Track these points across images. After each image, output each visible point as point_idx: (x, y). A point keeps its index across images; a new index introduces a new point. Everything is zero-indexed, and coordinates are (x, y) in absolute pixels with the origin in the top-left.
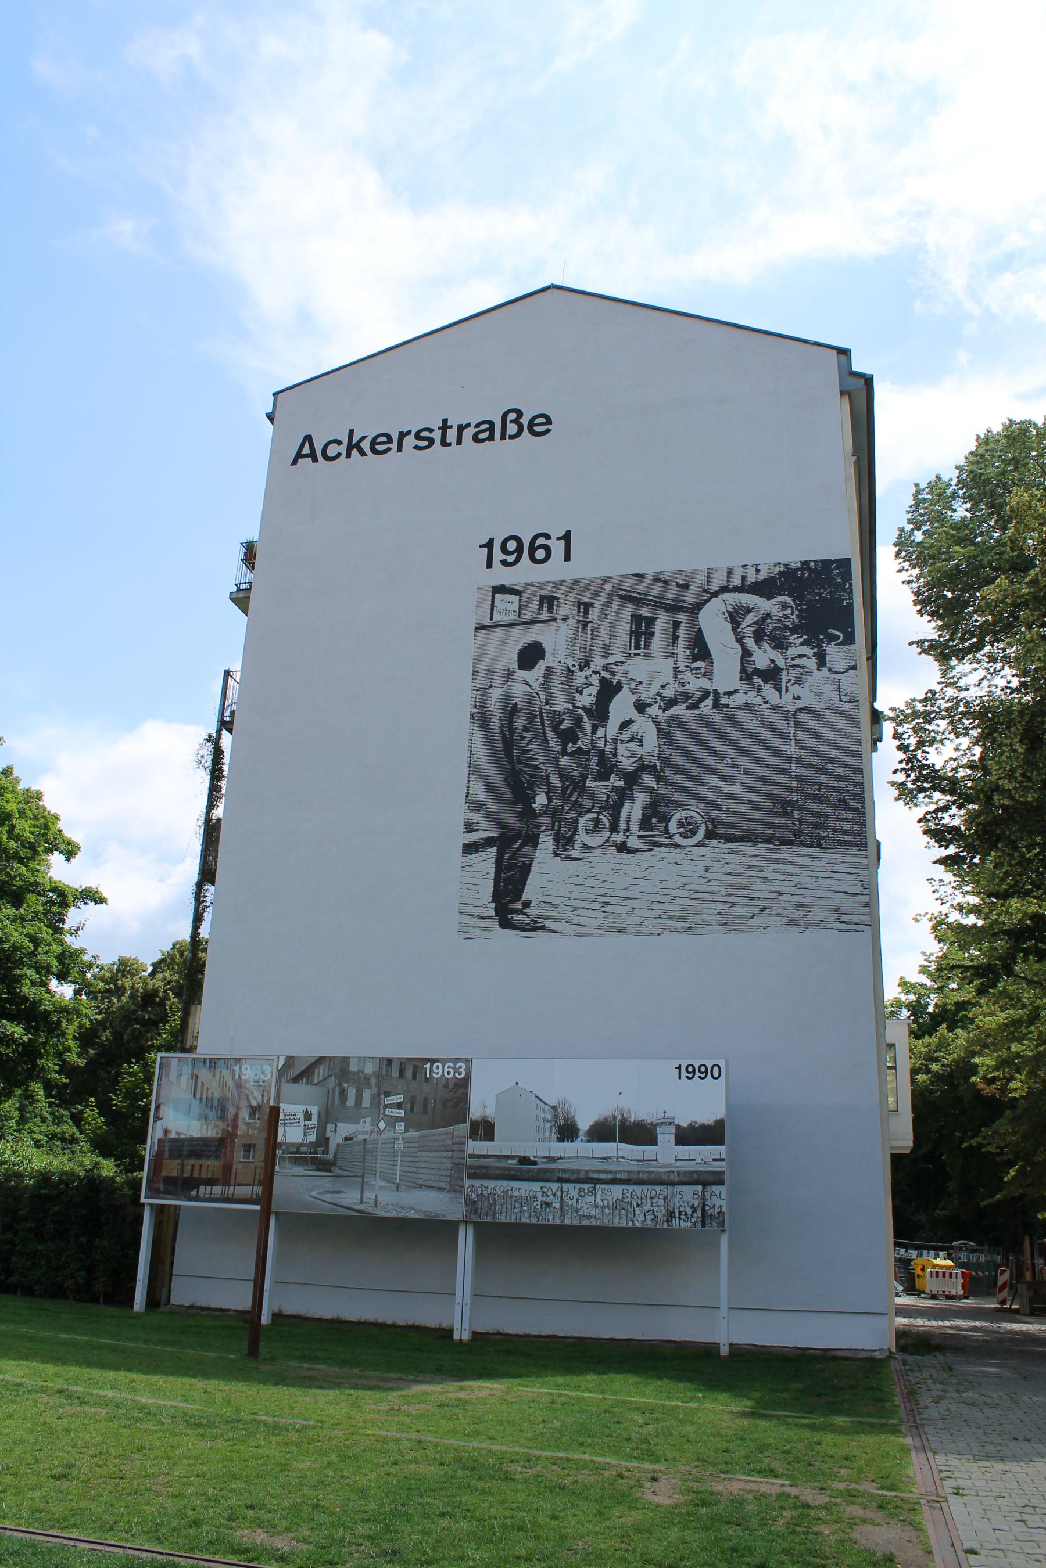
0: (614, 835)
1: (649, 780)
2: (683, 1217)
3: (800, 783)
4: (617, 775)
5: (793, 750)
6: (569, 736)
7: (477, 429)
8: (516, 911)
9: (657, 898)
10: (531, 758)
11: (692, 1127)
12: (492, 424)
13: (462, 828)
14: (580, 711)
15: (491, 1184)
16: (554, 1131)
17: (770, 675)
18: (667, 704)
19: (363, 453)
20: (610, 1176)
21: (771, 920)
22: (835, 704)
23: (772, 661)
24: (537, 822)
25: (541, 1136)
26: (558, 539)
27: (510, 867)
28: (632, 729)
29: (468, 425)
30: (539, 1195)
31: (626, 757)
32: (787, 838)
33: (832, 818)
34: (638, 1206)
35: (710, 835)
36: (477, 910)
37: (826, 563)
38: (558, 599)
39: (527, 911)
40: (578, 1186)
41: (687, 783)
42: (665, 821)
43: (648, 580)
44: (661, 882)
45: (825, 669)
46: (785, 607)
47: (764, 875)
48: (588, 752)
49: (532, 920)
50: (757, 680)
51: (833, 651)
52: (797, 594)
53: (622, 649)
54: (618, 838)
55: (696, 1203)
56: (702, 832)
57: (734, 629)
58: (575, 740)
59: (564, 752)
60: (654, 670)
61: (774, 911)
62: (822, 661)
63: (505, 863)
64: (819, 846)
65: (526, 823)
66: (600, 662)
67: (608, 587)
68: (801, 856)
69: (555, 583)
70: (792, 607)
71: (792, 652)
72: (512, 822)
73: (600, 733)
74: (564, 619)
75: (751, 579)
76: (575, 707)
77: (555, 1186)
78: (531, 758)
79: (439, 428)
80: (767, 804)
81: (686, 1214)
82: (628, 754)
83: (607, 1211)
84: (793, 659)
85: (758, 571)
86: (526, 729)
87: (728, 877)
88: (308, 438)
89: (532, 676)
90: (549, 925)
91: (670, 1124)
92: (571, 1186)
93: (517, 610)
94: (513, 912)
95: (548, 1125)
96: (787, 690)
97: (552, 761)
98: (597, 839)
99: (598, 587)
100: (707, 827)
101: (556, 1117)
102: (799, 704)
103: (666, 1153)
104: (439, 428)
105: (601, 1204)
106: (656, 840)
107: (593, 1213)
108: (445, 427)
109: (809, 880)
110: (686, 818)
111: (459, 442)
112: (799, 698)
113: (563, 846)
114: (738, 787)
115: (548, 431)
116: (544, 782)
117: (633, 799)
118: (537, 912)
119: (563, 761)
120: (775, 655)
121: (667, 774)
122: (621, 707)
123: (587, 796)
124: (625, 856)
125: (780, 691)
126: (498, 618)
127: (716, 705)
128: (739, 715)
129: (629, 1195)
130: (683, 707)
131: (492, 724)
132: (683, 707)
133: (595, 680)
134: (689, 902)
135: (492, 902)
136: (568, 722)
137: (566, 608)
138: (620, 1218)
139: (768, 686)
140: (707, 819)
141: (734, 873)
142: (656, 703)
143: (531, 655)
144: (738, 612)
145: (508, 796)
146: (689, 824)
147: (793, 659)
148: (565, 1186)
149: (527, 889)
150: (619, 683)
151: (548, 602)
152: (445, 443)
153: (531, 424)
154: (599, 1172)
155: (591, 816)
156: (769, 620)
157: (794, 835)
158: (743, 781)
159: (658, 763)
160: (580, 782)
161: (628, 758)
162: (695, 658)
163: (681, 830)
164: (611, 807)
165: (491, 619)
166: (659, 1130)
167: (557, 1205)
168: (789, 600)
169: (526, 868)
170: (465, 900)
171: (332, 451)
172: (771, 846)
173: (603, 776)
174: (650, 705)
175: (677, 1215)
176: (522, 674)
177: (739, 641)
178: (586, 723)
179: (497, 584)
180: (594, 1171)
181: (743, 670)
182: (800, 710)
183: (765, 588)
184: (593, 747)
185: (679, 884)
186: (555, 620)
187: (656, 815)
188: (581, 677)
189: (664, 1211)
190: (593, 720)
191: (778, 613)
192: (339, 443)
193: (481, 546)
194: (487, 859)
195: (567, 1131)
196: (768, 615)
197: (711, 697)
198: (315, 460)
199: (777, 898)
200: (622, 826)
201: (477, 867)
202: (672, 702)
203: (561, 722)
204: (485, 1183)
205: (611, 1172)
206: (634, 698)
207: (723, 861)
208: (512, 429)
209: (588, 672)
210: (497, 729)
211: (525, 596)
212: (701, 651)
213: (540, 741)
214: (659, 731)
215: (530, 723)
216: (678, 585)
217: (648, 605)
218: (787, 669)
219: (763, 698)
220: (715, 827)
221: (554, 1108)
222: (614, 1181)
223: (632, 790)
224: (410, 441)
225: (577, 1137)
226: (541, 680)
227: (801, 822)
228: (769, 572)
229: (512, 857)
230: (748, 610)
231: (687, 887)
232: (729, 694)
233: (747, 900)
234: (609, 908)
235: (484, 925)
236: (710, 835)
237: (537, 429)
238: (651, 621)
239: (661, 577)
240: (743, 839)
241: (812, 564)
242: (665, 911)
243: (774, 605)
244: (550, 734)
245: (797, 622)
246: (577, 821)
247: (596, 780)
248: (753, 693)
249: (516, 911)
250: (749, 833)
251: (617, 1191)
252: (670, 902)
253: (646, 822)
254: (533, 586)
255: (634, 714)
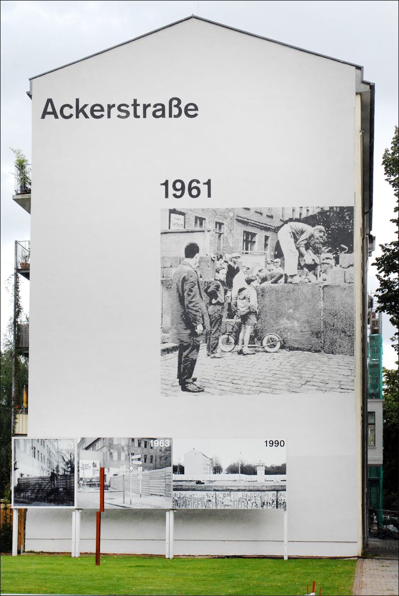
0: (237, 346)
1: (253, 319)
3: (325, 322)
4: (237, 316)
5: (322, 306)
6: (213, 295)
7: (155, 109)
8: (190, 383)
9: (257, 377)
10: (194, 306)
13: (160, 341)
14: (218, 282)
17: (312, 267)
18: (262, 280)
19: (86, 117)
21: (310, 387)
22: (343, 284)
23: (313, 260)
24: (198, 339)
26: (204, 184)
27: (186, 361)
28: (244, 293)
29: (149, 105)
31: (242, 308)
32: (318, 349)
33: (339, 340)
35: (282, 347)
36: (170, 382)
37: (342, 208)
38: (205, 219)
39: (195, 383)
41: (272, 321)
42: (261, 339)
43: (252, 211)
44: (259, 369)
45: (338, 266)
46: (321, 231)
47: (307, 366)
48: (222, 304)
49: (198, 387)
50: (306, 270)
51: (342, 256)
52: (327, 225)
53: (239, 250)
54: (238, 348)
56: (278, 345)
57: (295, 242)
58: (216, 297)
59: (210, 303)
60: (255, 262)
61: (311, 383)
62: (337, 262)
63: (183, 359)
64: (333, 353)
65: (193, 339)
66: (227, 257)
67: (231, 214)
68: (323, 357)
69: (203, 210)
70: (324, 232)
71: (323, 256)
72: (186, 339)
73: (229, 294)
74: (208, 231)
75: (304, 215)
76: (215, 280)
78: (194, 306)
79: (132, 105)
80: (309, 333)
82: (243, 306)
84: (323, 260)
85: (308, 210)
86: (191, 291)
87: (291, 367)
88: (50, 101)
89: (193, 261)
90: (206, 389)
93: (183, 224)
94: (188, 383)
96: (320, 276)
97: (204, 308)
98: (228, 348)
99: (226, 214)
100: (281, 343)
102: (326, 283)
104: (132, 105)
106: (257, 349)
109: (327, 369)
110: (271, 338)
111: (145, 116)
112: (325, 280)
113: (212, 351)
114: (296, 324)
115: (196, 115)
116: (201, 319)
117: (245, 329)
118: (200, 383)
119: (211, 308)
120: (315, 257)
121: (262, 316)
122: (239, 281)
123: (223, 326)
124: (241, 356)
125: (316, 276)
126: (173, 229)
127: (286, 282)
128: (297, 287)
130: (270, 282)
131: (172, 287)
132: (270, 282)
133: (225, 266)
134: (272, 379)
135: (178, 378)
136: (212, 288)
137: (209, 225)
139: (311, 273)
140: (281, 339)
141: (293, 366)
142: (256, 279)
143: (192, 250)
144: (297, 233)
145: (183, 326)
146: (272, 341)
147: (323, 260)
149: (194, 372)
150: (238, 268)
151: (200, 220)
155: (225, 336)
156: (312, 238)
157: (321, 348)
158: (298, 321)
159: (257, 311)
160: (219, 319)
161: (243, 307)
162: (276, 257)
163: (269, 344)
164: (235, 332)
165: (169, 228)
168: (322, 228)
169: (194, 362)
170: (163, 377)
171: (67, 111)
172: (310, 353)
173: (231, 316)
174: (253, 281)
176: (188, 260)
177: (298, 248)
178: (222, 289)
179: (172, 208)
181: (299, 264)
182: (326, 286)
183: (311, 220)
184: (225, 301)
185: (268, 370)
186: (204, 231)
187: (256, 336)
188: (218, 264)
190: (225, 287)
191: (317, 235)
192: (71, 107)
194: (174, 357)
196: (312, 236)
197: (284, 278)
198: (56, 117)
199: (313, 377)
200: (240, 342)
201: (168, 361)
202: (264, 280)
203: (209, 287)
206: (245, 277)
207: (288, 360)
208: (175, 111)
209: (221, 261)
210: (175, 290)
211: (187, 216)
212: (279, 253)
213: (198, 297)
214: (258, 294)
215: (193, 287)
216: (268, 216)
217: (252, 226)
218: (320, 265)
219: (308, 279)
220: (285, 343)
223: (245, 324)
224: (114, 111)
226: (198, 264)
227: (324, 342)
228: (313, 212)
229: (187, 356)
230: (302, 232)
231: (272, 372)
232: (292, 276)
233: (299, 378)
234: (234, 382)
235: (173, 390)
236: (282, 347)
238: (254, 235)
239: (259, 211)
240: (297, 349)
241: (335, 209)
242: (261, 383)
243: (315, 230)
244: (204, 294)
245: (326, 240)
246: (218, 339)
247: (227, 318)
248: (304, 277)
249: (190, 383)
250: (300, 346)
252: (263, 379)
253: (252, 339)
254: (192, 210)
255: (245, 285)
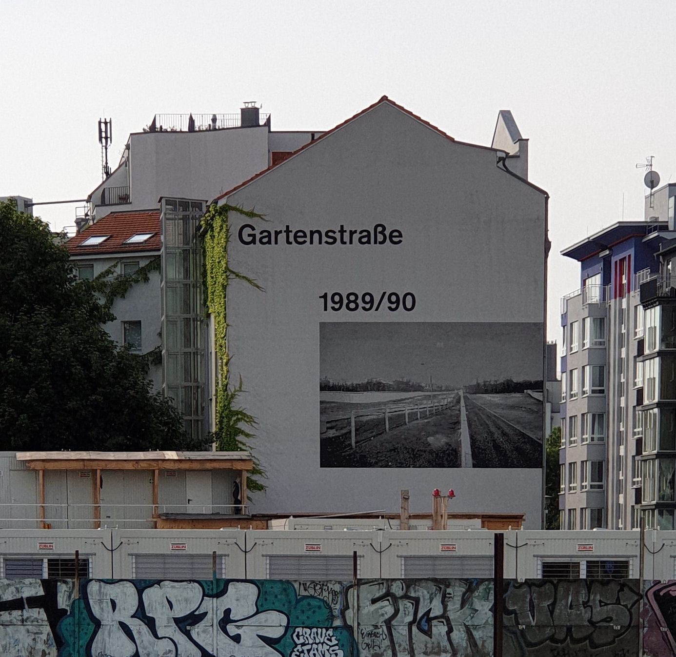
12: (368, 232)
29: (356, 232)
79: (339, 231)
104: (339, 231)
108: (342, 231)
115: (400, 242)
152: (343, 243)
153: (391, 236)
193: (320, 297)
208: (380, 238)
237: (395, 239)
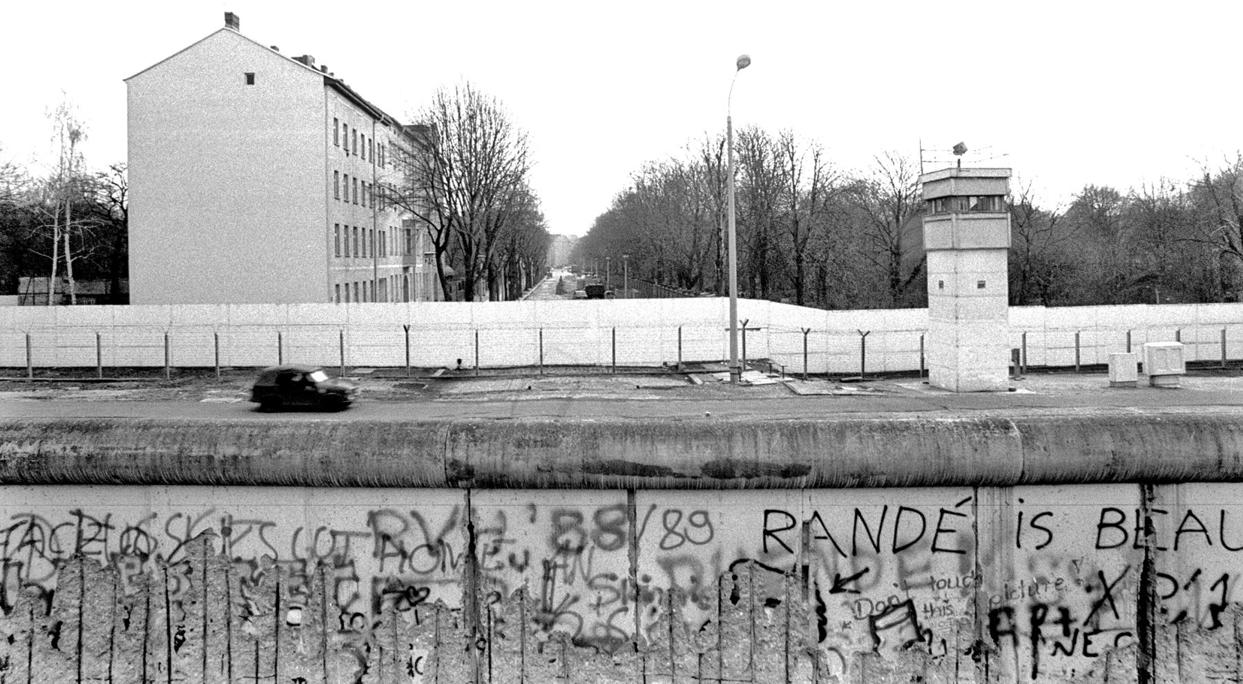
2: (1051, 631)
11: (1094, 213)
15: (123, 506)
16: (424, 245)
20: (704, 454)
25: (362, 269)
30: (363, 553)
34: (838, 586)
40: (549, 502)
55: (1112, 564)
77: (438, 508)
81: (1065, 619)
83: (691, 613)
91: (986, 202)
92: (512, 503)
95: (394, 219)
101: (431, 175)
103: (968, 331)
105: (660, 580)
107: (626, 623)
129: (793, 537)
138: (757, 645)
148: (487, 504)
154: (649, 433)
166: (933, 232)
167: (451, 595)
175: (1023, 620)
180: (626, 432)
189: (961, 606)
195: (485, 248)
204: (95, 501)
205: (706, 433)
221: (422, 136)
222: (722, 477)
225: (537, 273)
251: (738, 521)
